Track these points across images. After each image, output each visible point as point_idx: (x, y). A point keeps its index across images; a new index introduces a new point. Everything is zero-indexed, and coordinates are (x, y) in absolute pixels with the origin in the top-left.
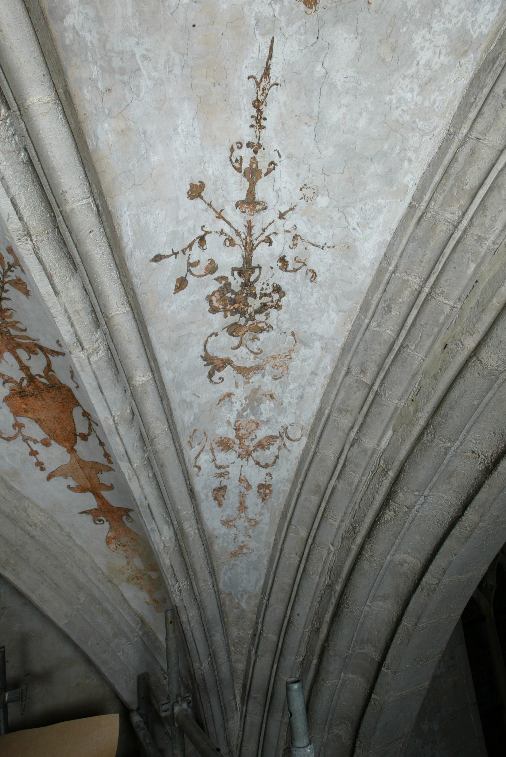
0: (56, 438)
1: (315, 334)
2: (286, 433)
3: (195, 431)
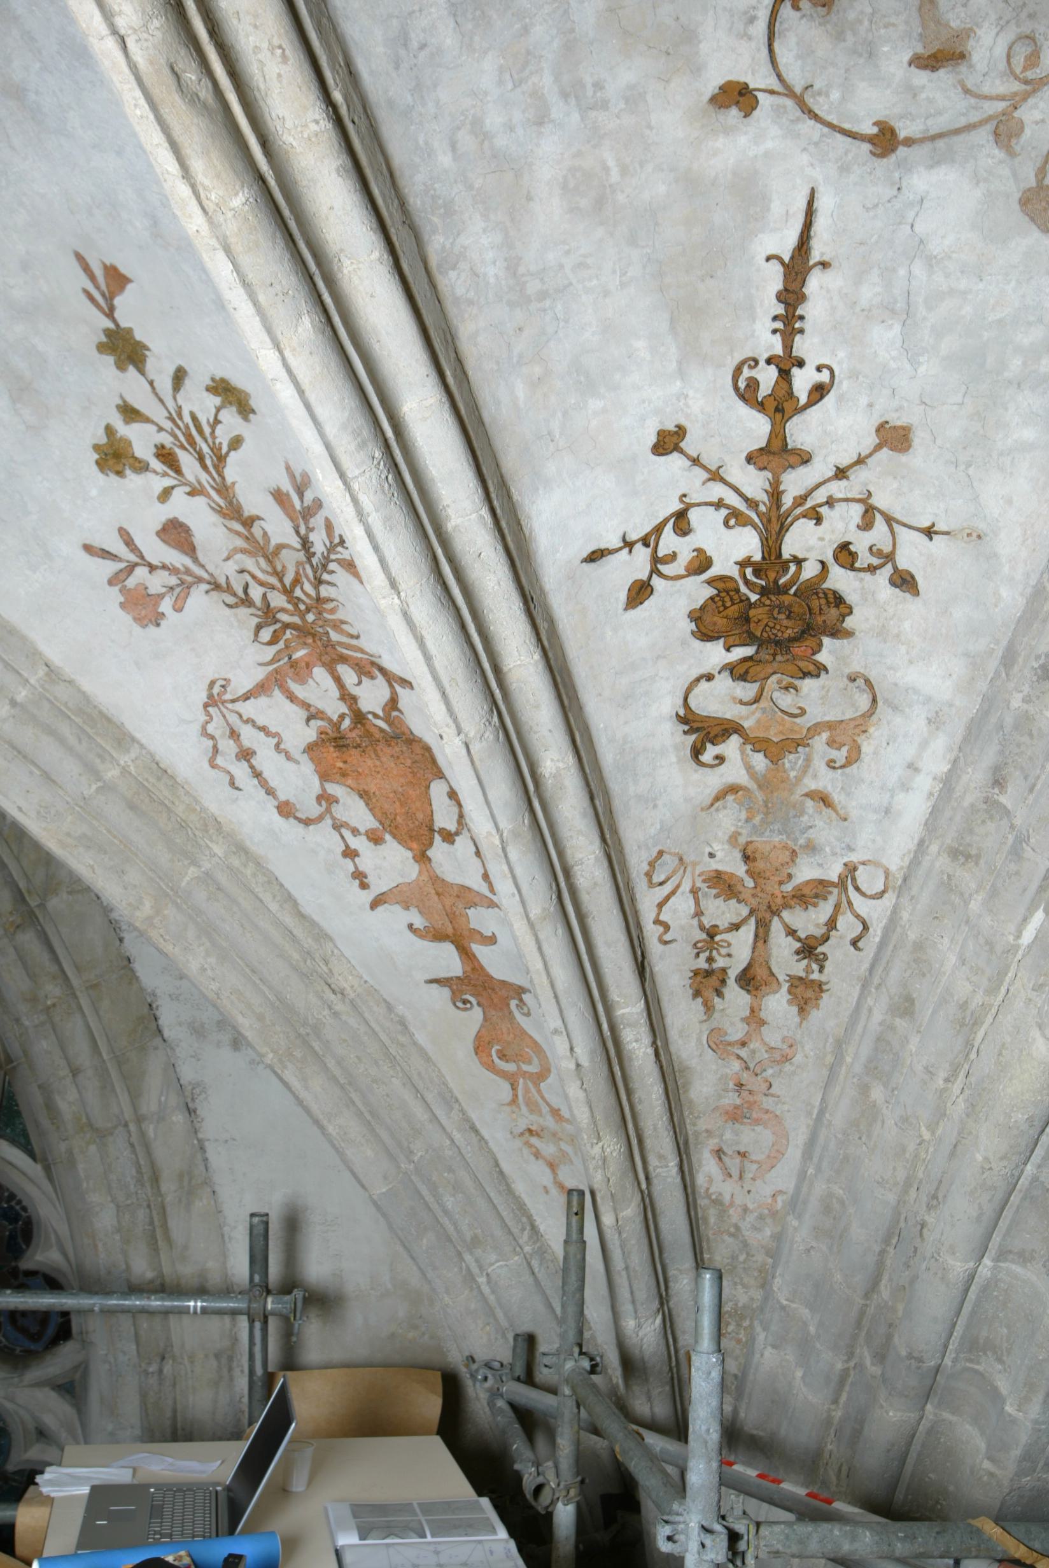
0: (394, 831)
1: (916, 691)
2: (854, 879)
3: (661, 853)
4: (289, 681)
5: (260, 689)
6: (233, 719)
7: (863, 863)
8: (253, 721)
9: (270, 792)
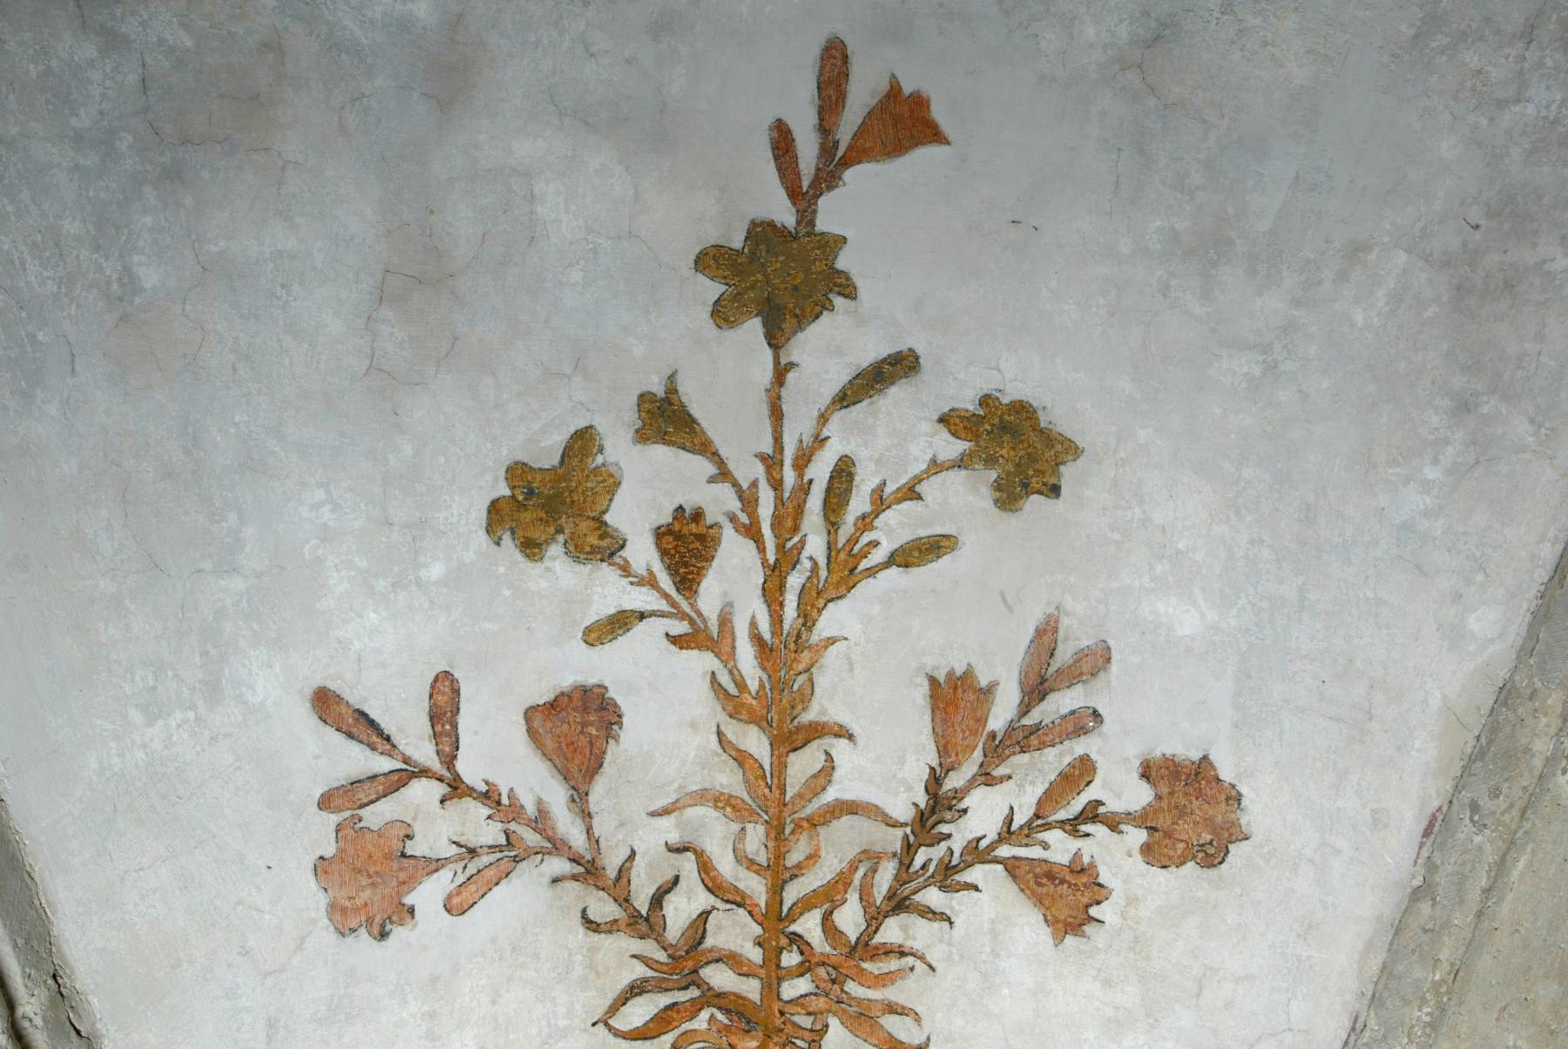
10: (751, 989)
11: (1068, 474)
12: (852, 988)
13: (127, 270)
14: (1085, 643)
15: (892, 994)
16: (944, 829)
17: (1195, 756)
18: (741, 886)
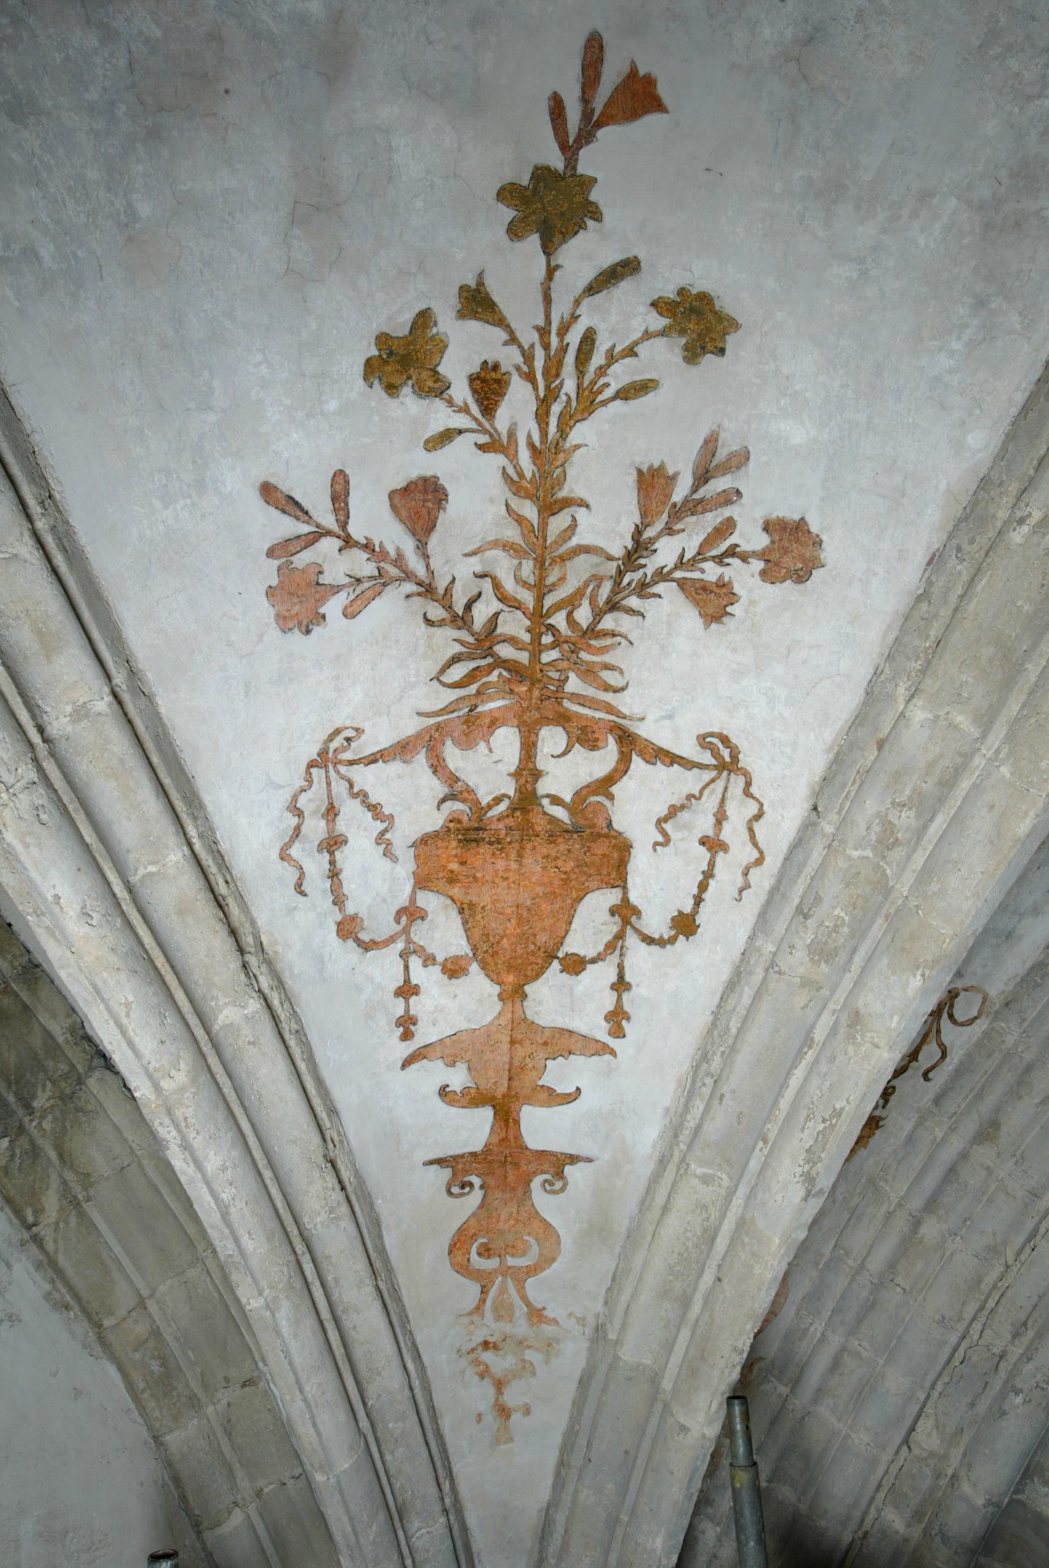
0: (489, 959)
2: (952, 1006)
4: (449, 742)
5: (402, 750)
6: (339, 788)
7: (966, 990)
8: (366, 795)
9: (339, 901)
10: (523, 657)
11: (731, 341)
12: (584, 656)
13: (129, 204)
14: (734, 448)
15: (607, 658)
16: (642, 561)
17: (797, 517)
18: (518, 597)
